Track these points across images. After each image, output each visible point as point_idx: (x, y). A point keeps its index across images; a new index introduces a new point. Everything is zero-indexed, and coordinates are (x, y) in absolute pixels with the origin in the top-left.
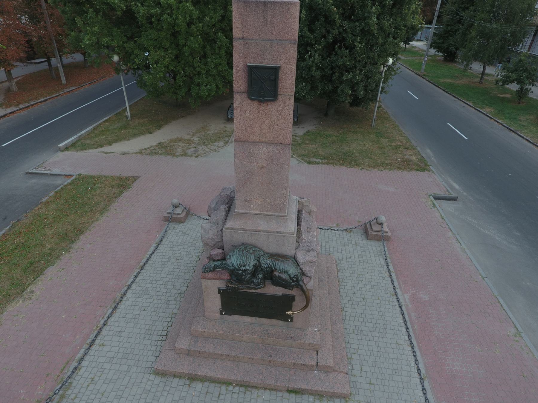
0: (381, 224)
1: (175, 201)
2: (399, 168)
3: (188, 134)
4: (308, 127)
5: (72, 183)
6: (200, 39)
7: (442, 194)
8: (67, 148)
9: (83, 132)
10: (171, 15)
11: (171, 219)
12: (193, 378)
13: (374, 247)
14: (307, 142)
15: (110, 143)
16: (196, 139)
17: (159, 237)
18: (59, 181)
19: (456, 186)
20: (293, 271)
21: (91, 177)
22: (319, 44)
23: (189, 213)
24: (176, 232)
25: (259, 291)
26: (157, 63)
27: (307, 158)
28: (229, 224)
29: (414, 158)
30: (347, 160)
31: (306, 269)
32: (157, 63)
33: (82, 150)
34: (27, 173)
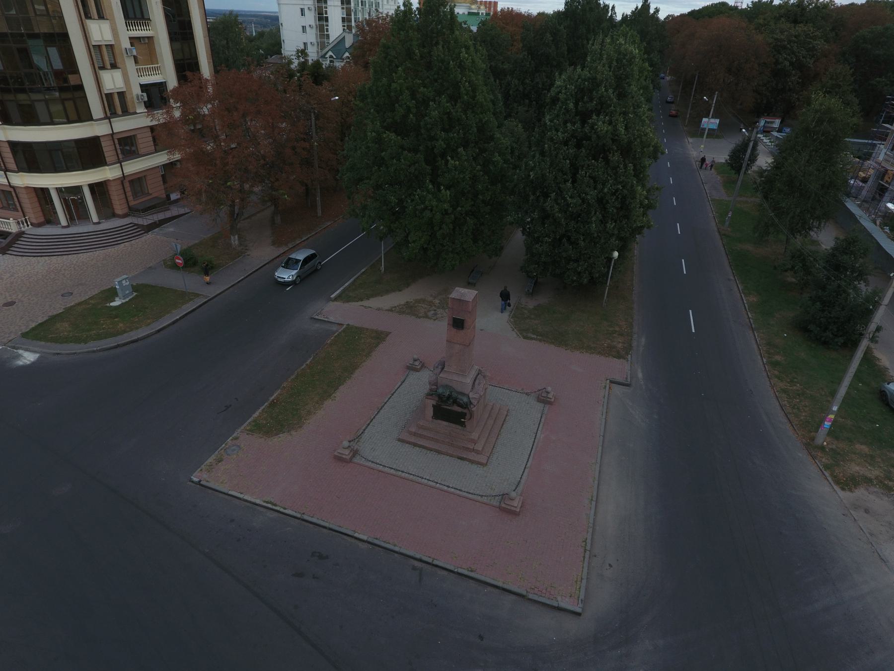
0: (548, 393)
1: (415, 357)
2: (599, 353)
3: (431, 296)
4: (542, 300)
5: (344, 331)
6: (451, 226)
7: (618, 378)
8: (336, 299)
9: (347, 284)
10: (431, 211)
11: (411, 368)
12: (415, 445)
13: (540, 406)
14: (533, 316)
15: (368, 299)
16: (437, 301)
17: (403, 379)
18: (334, 328)
19: (640, 375)
20: (465, 400)
21: (356, 328)
22: (549, 237)
23: (423, 366)
24: (413, 377)
25: (450, 409)
26: (414, 242)
27: (524, 332)
28: (441, 375)
29: (620, 345)
30: (558, 339)
31: (473, 401)
32: (414, 242)
33: (348, 301)
34: (312, 318)
